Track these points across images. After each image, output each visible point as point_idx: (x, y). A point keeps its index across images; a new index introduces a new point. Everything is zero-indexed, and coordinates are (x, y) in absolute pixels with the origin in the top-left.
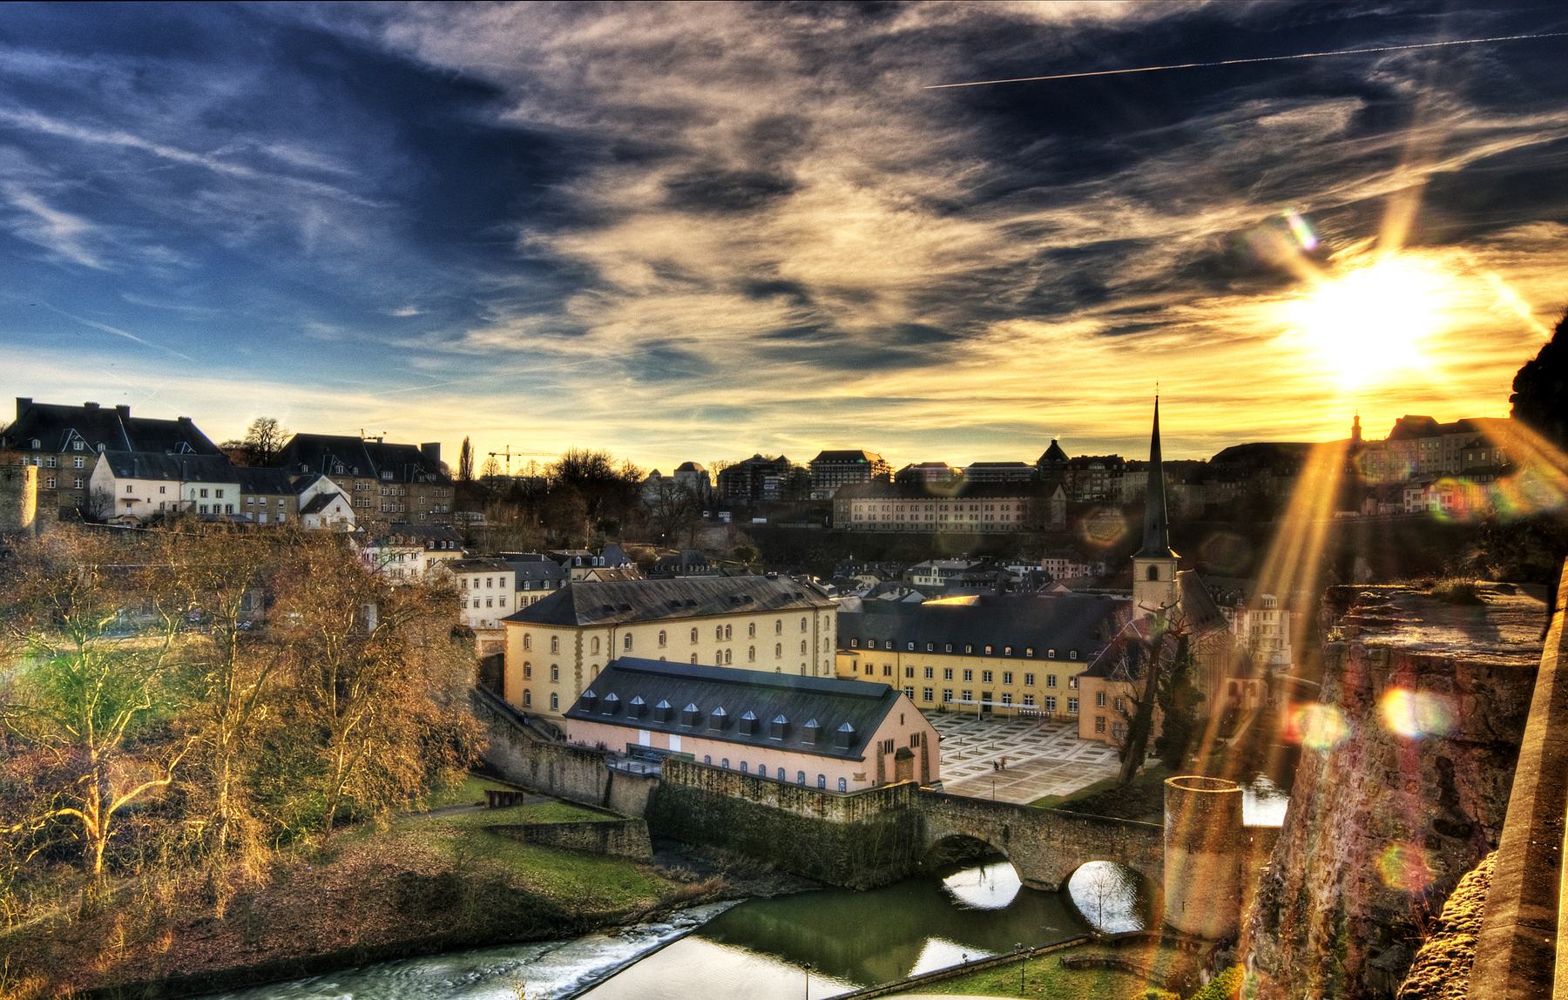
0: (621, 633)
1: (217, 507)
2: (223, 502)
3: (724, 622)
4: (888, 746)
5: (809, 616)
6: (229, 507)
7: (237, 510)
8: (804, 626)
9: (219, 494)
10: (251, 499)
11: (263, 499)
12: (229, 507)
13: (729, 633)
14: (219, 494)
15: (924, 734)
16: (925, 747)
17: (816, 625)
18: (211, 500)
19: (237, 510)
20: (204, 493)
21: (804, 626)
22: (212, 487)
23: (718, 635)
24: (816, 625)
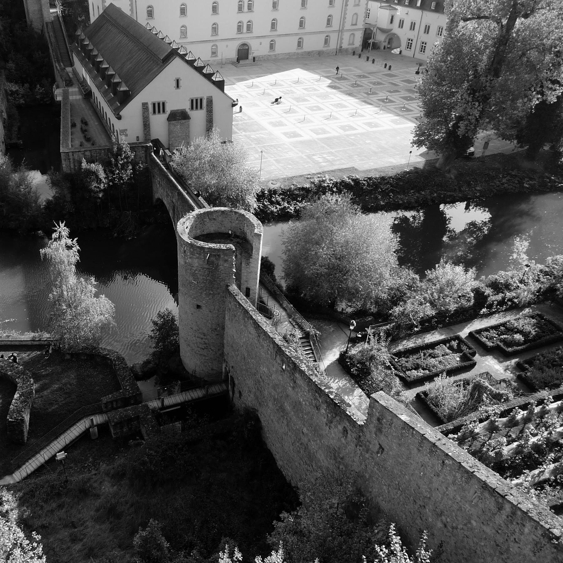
4: (159, 107)
15: (210, 102)
16: (210, 111)
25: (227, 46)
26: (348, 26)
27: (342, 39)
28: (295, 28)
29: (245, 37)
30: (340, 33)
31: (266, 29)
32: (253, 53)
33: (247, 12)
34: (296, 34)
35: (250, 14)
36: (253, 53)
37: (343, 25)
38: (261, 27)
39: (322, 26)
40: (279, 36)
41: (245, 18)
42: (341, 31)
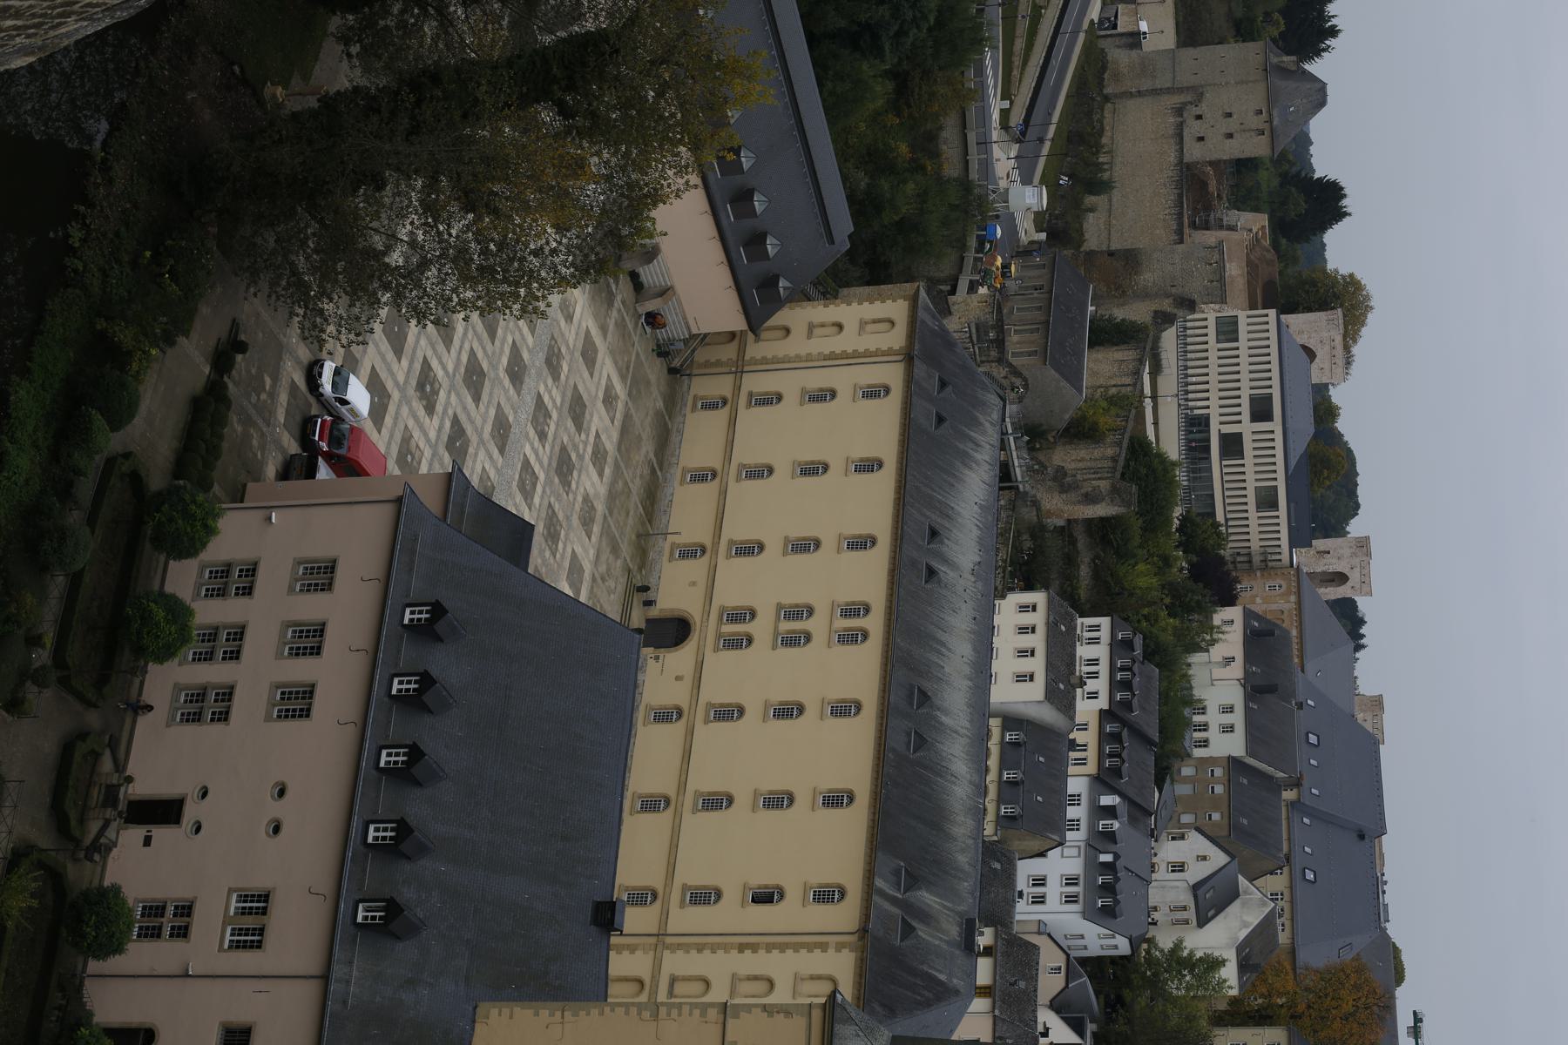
0: (892, 375)
1: (1204, 727)
2: (1213, 734)
3: (874, 623)
5: (844, 917)
6: (1205, 743)
7: (1198, 753)
8: (826, 895)
9: (1229, 729)
10: (1218, 772)
11: (1219, 789)
12: (1205, 743)
13: (852, 638)
14: (1229, 729)
17: (815, 942)
18: (1213, 718)
19: (1198, 753)
20: (1229, 709)
21: (826, 895)
22: (1237, 719)
23: (855, 610)
24: (815, 942)
25: (694, 584)
26: (675, 963)
27: (632, 949)
28: (704, 780)
29: (706, 631)
30: (653, 940)
31: (716, 691)
32: (657, 658)
33: (776, 628)
34: (682, 785)
35: (769, 638)
36: (657, 658)
37: (686, 948)
38: (727, 676)
39: (692, 873)
40: (690, 732)
41: (760, 628)
42: (661, 939)
